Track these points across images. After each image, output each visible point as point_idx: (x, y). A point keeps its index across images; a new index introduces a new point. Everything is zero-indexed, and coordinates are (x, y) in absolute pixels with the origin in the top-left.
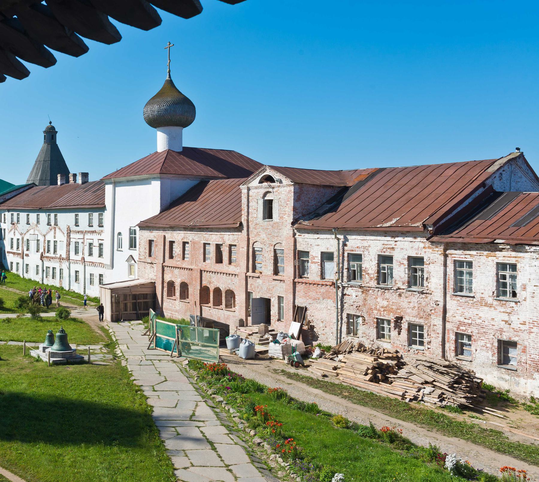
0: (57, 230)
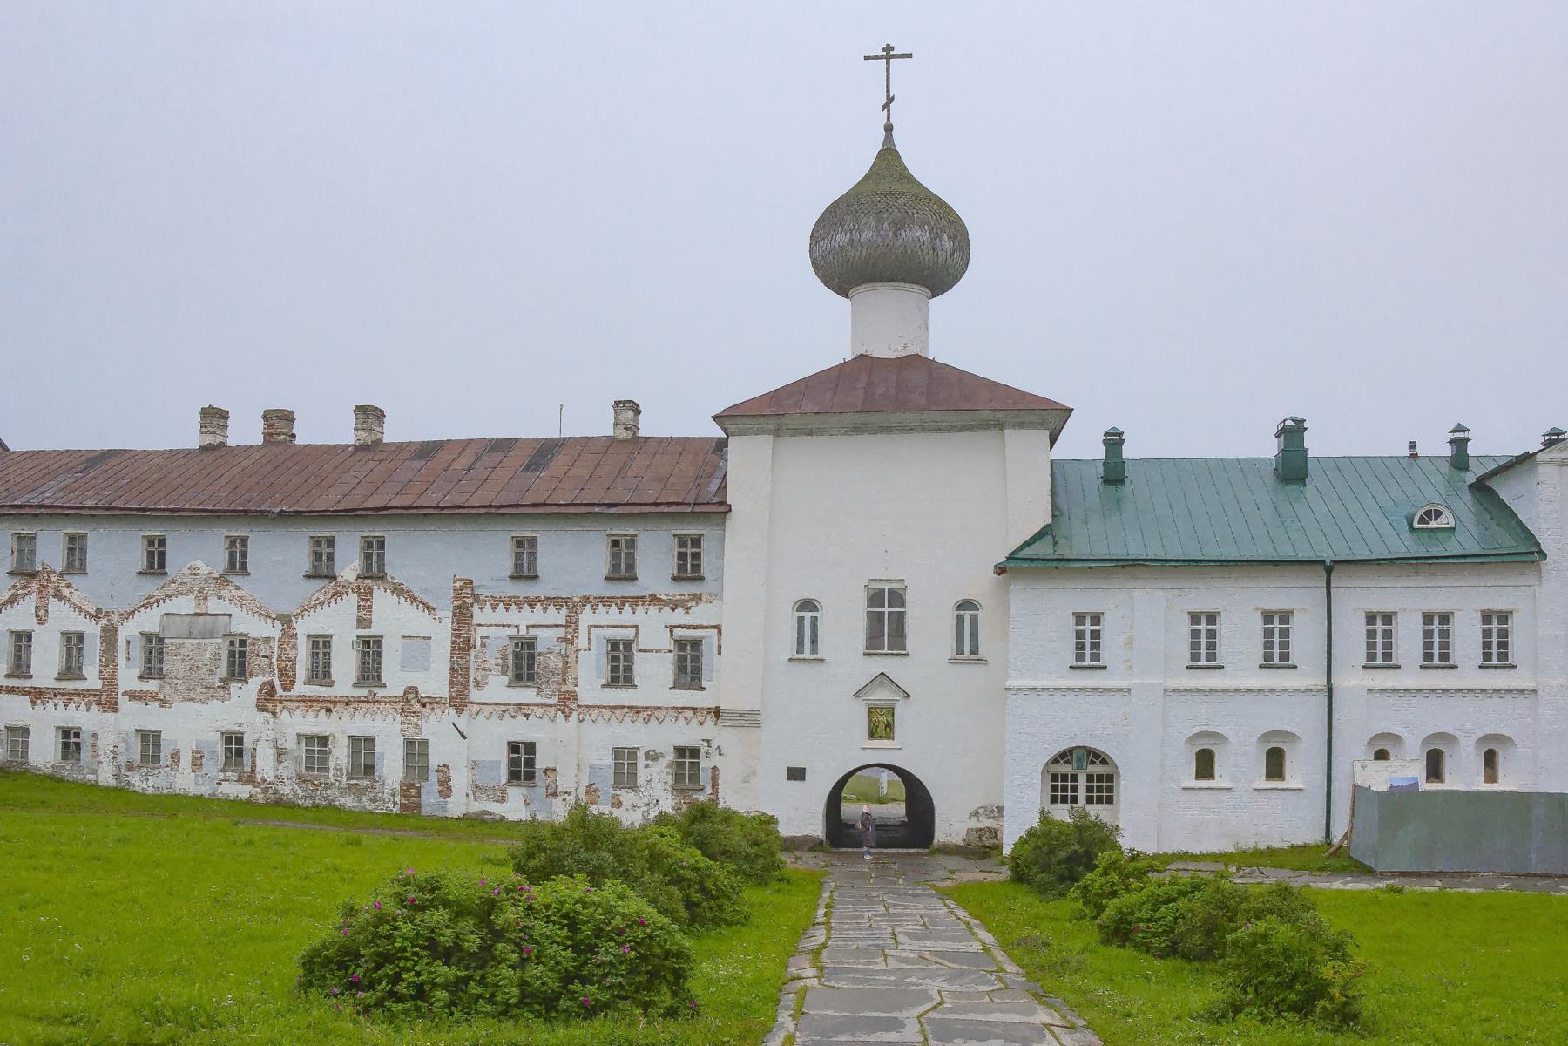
0: (383, 600)
